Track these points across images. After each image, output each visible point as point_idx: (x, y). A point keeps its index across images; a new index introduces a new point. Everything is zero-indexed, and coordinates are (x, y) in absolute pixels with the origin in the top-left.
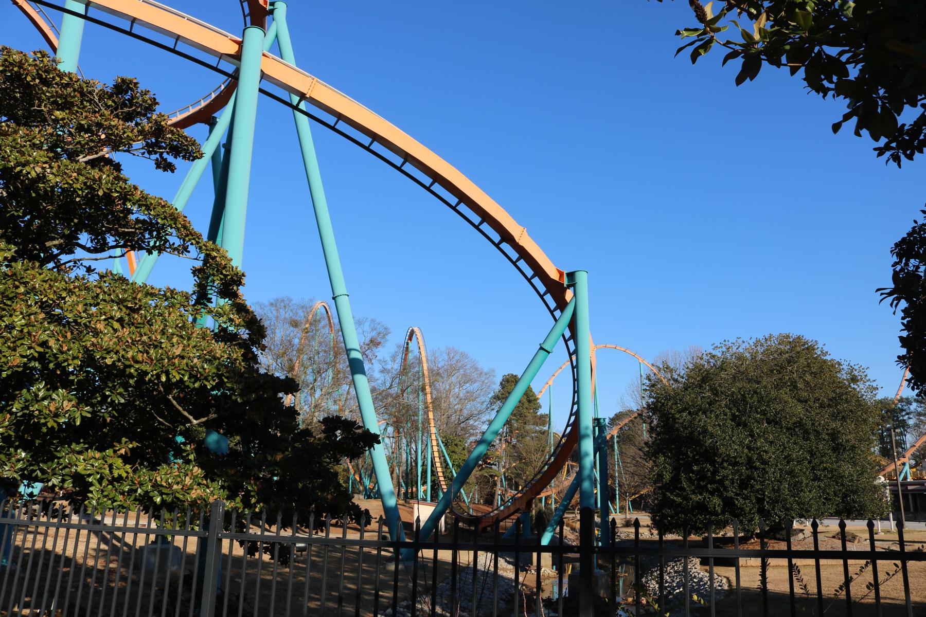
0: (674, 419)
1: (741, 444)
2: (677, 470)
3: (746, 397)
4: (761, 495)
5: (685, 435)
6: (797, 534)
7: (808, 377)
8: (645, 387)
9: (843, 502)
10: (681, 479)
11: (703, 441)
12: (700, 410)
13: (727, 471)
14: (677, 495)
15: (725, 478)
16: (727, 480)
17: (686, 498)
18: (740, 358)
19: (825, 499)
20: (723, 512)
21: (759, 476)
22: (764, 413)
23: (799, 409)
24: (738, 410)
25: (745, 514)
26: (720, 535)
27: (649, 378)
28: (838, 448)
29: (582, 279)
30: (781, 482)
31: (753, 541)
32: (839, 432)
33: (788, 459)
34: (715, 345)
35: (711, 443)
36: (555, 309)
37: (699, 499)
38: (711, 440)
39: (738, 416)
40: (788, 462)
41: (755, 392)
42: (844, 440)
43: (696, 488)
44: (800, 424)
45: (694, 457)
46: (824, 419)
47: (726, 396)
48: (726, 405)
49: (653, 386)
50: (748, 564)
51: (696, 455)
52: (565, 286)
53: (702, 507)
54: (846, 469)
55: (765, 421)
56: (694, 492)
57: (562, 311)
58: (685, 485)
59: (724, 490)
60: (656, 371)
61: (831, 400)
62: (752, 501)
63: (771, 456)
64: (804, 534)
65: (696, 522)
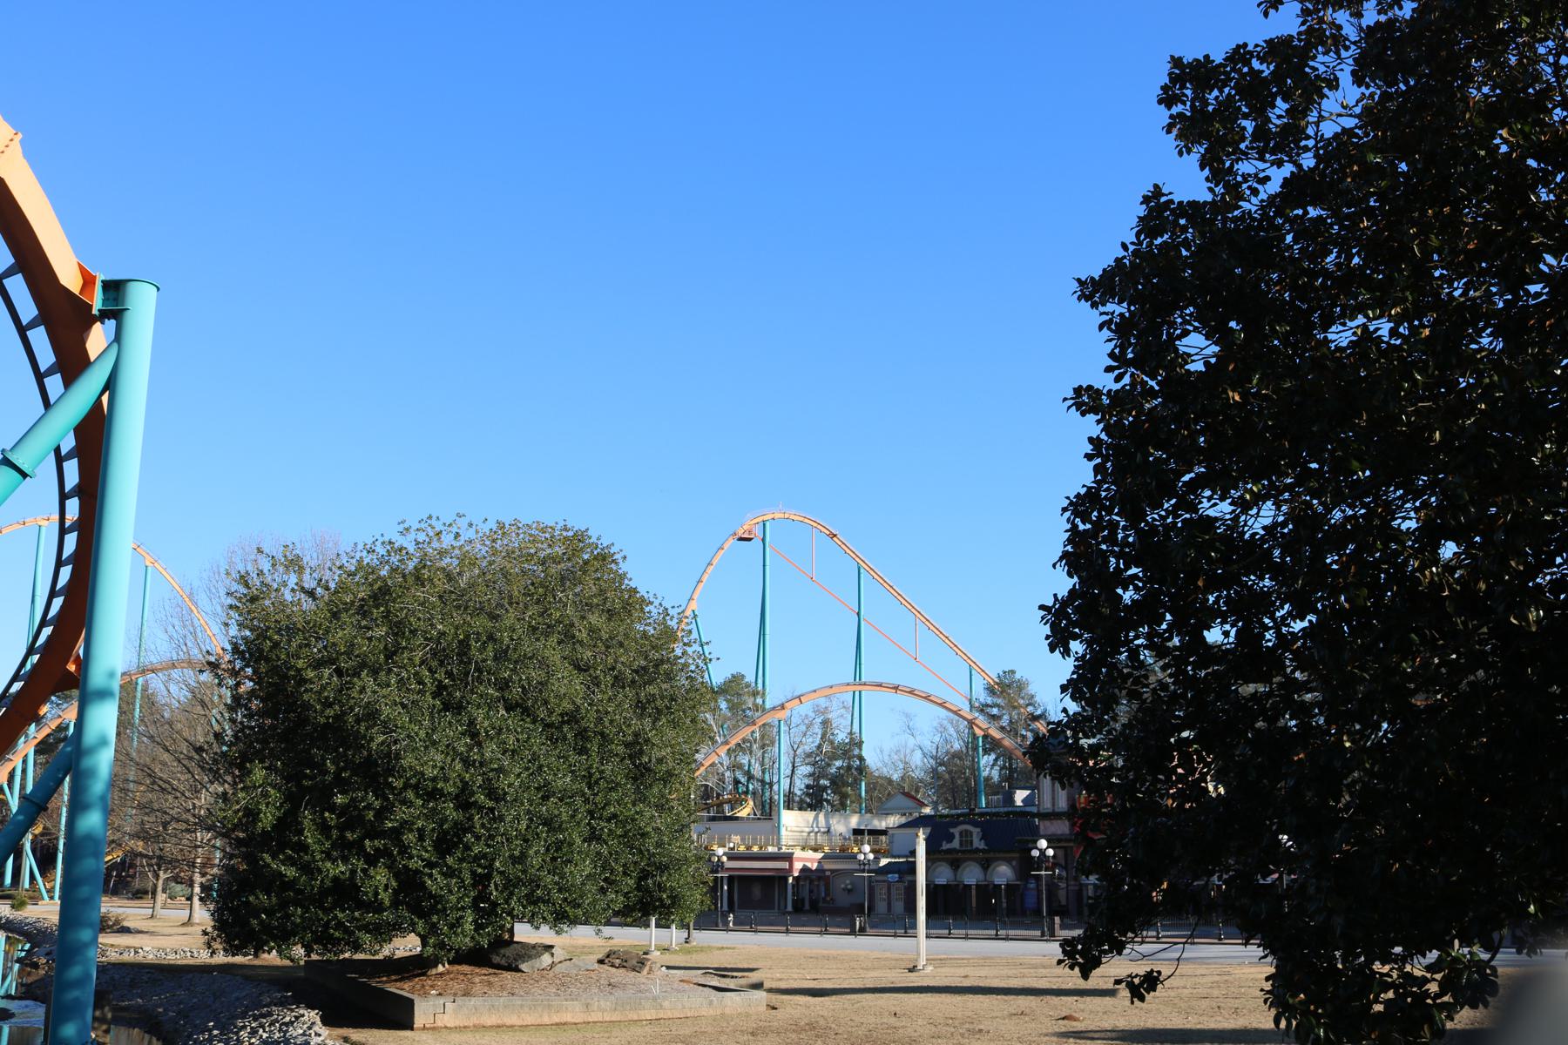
0: (302, 681)
1: (450, 749)
2: (293, 801)
3: (469, 647)
4: (484, 868)
5: (323, 720)
6: (539, 955)
7: (595, 619)
8: (230, 601)
9: (639, 888)
10: (302, 823)
11: (364, 737)
12: (363, 665)
13: (410, 811)
14: (290, 861)
15: (406, 825)
16: (411, 830)
17: (308, 870)
18: (467, 560)
19: (606, 880)
20: (395, 903)
21: (483, 825)
22: (503, 685)
23: (578, 684)
24: (449, 674)
25: (445, 909)
26: (380, 957)
27: (244, 580)
28: (641, 774)
29: (143, 303)
30: (526, 841)
31: (440, 968)
32: (647, 741)
33: (546, 792)
34: (406, 525)
35: (383, 743)
36: (50, 372)
37: (342, 873)
38: (382, 738)
39: (445, 687)
40: (545, 798)
41: (491, 638)
42: (654, 760)
43: (334, 846)
44: (572, 717)
45: (337, 774)
46: (620, 711)
47: (426, 639)
48: (422, 663)
49: (253, 599)
50: (439, 1024)
51: (344, 769)
52: (95, 311)
53: (345, 892)
54: (651, 820)
55: (501, 705)
56: (328, 856)
57: (68, 382)
58: (309, 838)
59: (399, 853)
60: (266, 566)
61: (636, 672)
62: (463, 881)
63: (510, 783)
64: (552, 955)
65: (327, 926)
